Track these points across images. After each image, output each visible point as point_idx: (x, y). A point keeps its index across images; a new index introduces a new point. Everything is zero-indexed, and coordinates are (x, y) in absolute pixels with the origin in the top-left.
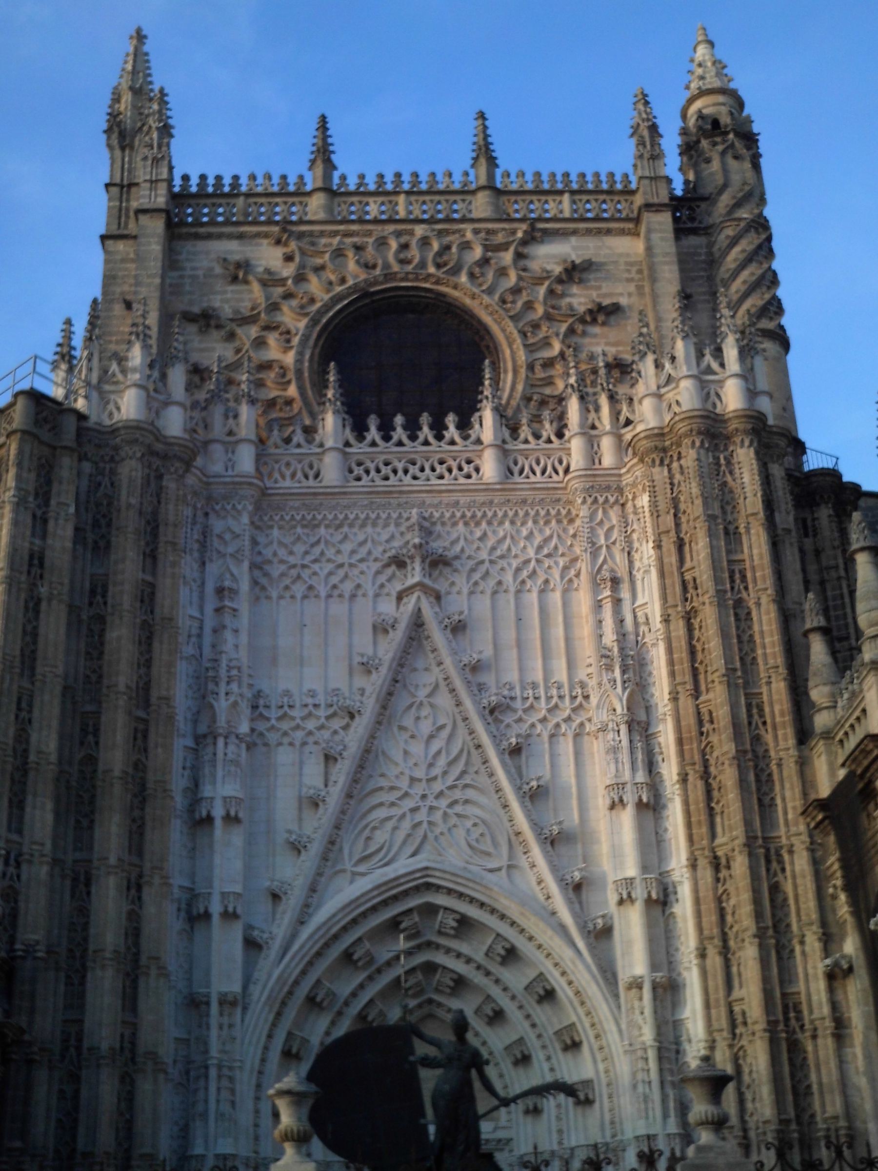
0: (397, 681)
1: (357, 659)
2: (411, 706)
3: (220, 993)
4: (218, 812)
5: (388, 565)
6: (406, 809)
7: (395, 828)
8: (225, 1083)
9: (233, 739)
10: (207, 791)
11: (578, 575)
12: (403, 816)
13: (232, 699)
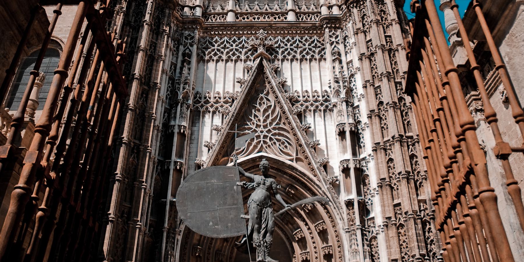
1: (236, 80)
4: (176, 130)
5: (250, 50)
10: (172, 123)
11: (325, 54)
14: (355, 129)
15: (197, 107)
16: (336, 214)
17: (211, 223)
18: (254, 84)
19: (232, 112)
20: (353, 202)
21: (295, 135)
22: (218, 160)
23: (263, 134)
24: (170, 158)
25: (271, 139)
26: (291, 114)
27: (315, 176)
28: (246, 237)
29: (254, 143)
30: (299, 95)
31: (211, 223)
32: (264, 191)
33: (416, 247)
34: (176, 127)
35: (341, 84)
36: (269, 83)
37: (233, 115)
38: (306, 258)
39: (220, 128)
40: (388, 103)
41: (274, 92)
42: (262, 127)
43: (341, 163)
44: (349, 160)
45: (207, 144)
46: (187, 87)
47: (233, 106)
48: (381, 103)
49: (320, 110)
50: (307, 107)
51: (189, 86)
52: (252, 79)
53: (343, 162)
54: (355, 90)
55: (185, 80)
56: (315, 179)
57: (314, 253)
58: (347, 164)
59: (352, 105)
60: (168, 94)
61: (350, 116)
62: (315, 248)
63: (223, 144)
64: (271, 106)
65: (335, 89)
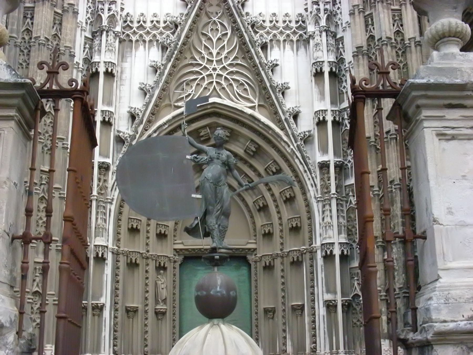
0: (201, 10)
2: (209, 23)
3: (99, 162)
4: (102, 70)
6: (204, 75)
7: (198, 84)
8: (102, 210)
9: (111, 34)
12: (203, 78)
13: (112, 13)
14: (336, 69)
15: (128, 35)
16: (307, 179)
20: (329, 165)
21: (259, 74)
23: (217, 72)
26: (253, 47)
29: (205, 84)
30: (264, 19)
33: (400, 223)
35: (322, 7)
39: (160, 64)
40: (381, 38)
41: (232, 15)
42: (215, 63)
43: (316, 114)
44: (326, 111)
45: (144, 86)
47: (176, 33)
48: (372, 37)
49: (292, 41)
50: (275, 35)
53: (318, 113)
54: (339, 16)
56: (281, 133)
58: (324, 115)
59: (334, 36)
60: (89, 18)
61: (330, 52)
62: (280, 218)
64: (227, 34)
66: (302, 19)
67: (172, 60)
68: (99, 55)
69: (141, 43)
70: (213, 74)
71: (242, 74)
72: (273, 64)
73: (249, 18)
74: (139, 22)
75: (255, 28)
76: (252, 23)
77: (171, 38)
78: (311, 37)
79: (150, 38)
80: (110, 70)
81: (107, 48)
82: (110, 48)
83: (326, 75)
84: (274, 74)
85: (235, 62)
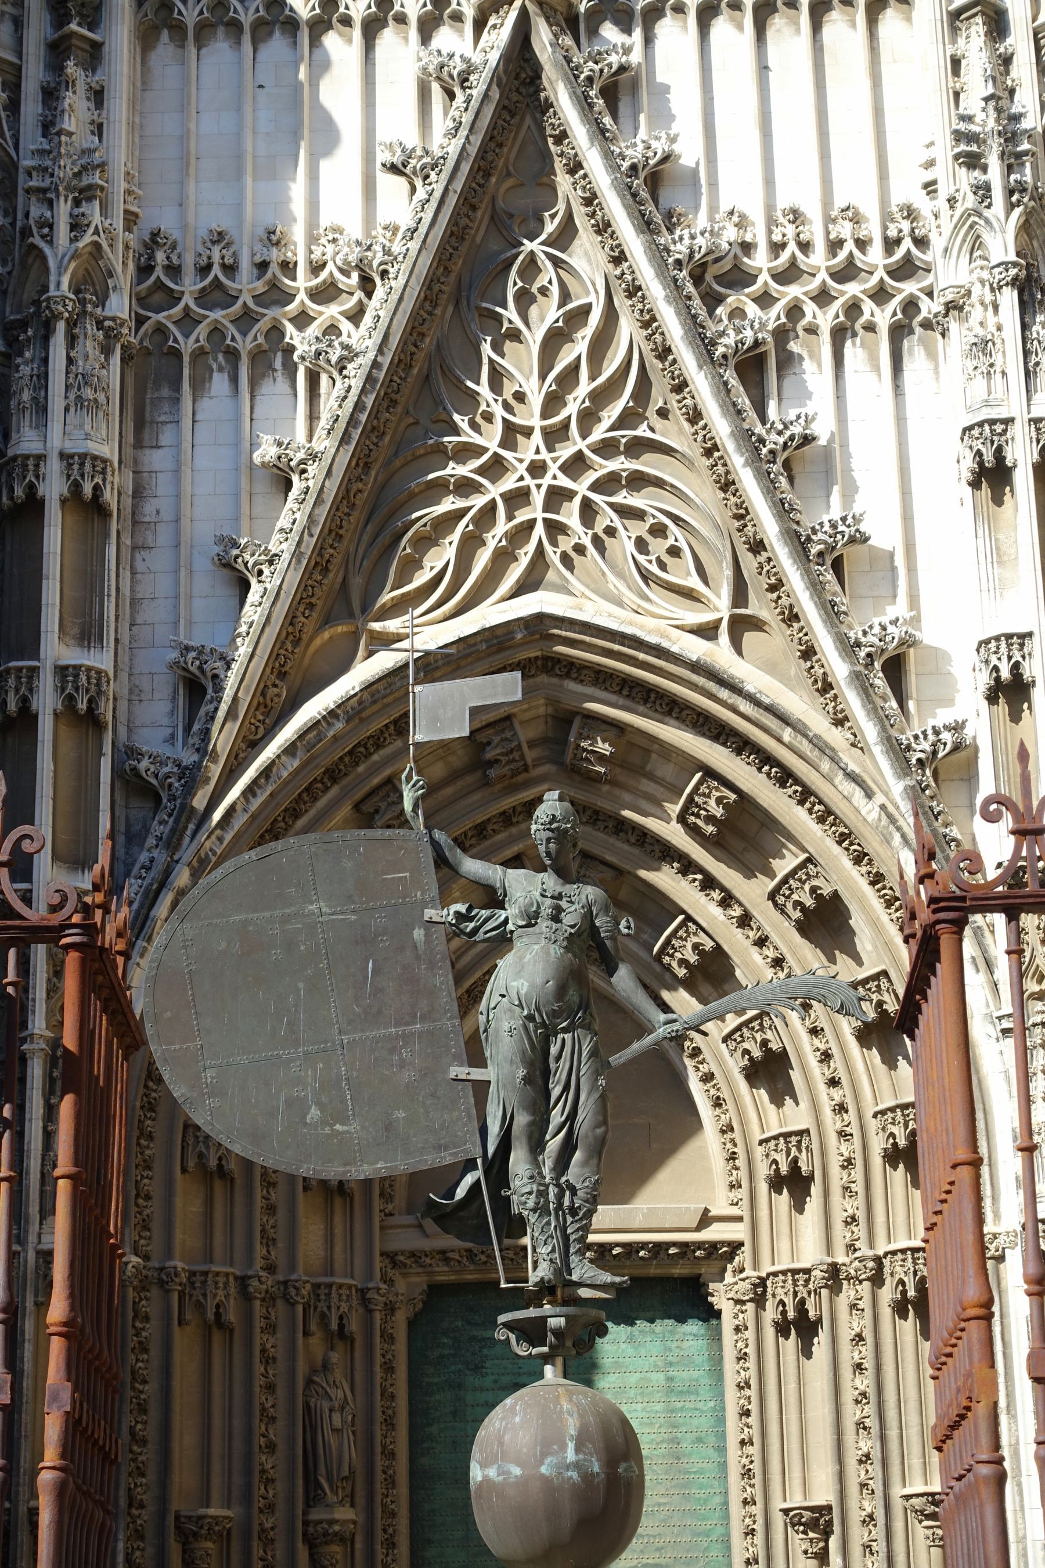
6: (494, 491)
12: (490, 508)
15: (161, 330)
17: (314, 1113)
18: (487, 175)
19: (366, 360)
21: (727, 485)
22: (297, 642)
23: (547, 481)
24: (32, 647)
25: (588, 511)
27: (839, 723)
28: (476, 1168)
31: (314, 1113)
32: (556, 951)
34: (54, 468)
36: (572, 172)
37: (370, 379)
38: (794, 1163)
39: (301, 455)
42: (537, 438)
46: (93, 212)
51: (105, 212)
52: (473, 150)
53: (993, 644)
55: (78, 175)
56: (836, 737)
57: (832, 1139)
58: (1017, 656)
63: (319, 549)
64: (585, 310)
65: (960, 209)
66: (913, 230)
67: (356, 434)
68: (37, 427)
69: (216, 360)
70: (534, 489)
71: (659, 483)
72: (792, 438)
73: (681, 238)
74: (204, 270)
75: (708, 277)
76: (697, 256)
77: (344, 338)
78: (952, 312)
79: (255, 338)
80: (88, 489)
81: (72, 396)
82: (88, 393)
83: (1024, 480)
84: (796, 481)
85: (625, 435)
